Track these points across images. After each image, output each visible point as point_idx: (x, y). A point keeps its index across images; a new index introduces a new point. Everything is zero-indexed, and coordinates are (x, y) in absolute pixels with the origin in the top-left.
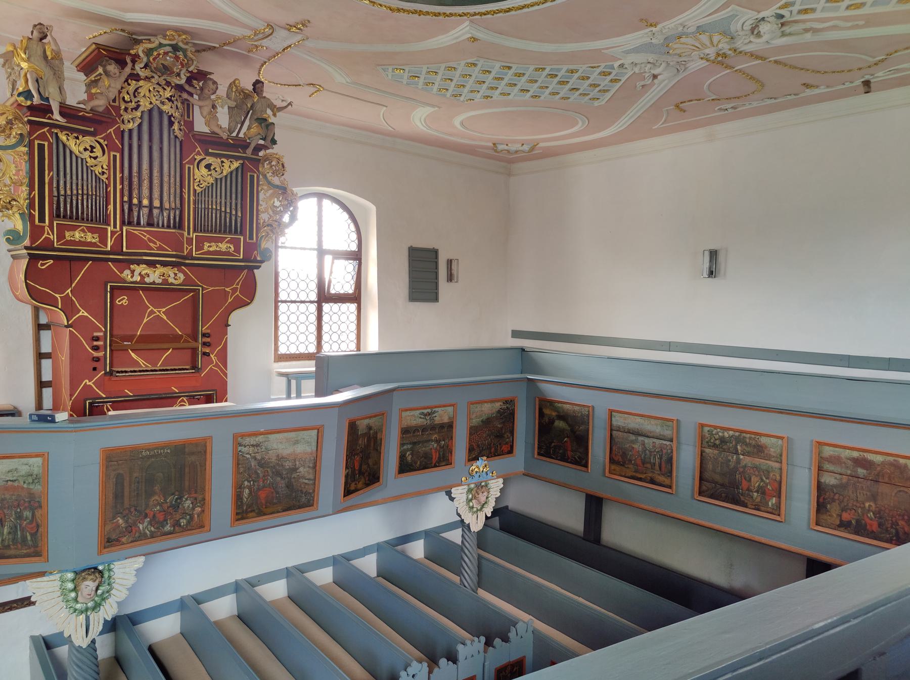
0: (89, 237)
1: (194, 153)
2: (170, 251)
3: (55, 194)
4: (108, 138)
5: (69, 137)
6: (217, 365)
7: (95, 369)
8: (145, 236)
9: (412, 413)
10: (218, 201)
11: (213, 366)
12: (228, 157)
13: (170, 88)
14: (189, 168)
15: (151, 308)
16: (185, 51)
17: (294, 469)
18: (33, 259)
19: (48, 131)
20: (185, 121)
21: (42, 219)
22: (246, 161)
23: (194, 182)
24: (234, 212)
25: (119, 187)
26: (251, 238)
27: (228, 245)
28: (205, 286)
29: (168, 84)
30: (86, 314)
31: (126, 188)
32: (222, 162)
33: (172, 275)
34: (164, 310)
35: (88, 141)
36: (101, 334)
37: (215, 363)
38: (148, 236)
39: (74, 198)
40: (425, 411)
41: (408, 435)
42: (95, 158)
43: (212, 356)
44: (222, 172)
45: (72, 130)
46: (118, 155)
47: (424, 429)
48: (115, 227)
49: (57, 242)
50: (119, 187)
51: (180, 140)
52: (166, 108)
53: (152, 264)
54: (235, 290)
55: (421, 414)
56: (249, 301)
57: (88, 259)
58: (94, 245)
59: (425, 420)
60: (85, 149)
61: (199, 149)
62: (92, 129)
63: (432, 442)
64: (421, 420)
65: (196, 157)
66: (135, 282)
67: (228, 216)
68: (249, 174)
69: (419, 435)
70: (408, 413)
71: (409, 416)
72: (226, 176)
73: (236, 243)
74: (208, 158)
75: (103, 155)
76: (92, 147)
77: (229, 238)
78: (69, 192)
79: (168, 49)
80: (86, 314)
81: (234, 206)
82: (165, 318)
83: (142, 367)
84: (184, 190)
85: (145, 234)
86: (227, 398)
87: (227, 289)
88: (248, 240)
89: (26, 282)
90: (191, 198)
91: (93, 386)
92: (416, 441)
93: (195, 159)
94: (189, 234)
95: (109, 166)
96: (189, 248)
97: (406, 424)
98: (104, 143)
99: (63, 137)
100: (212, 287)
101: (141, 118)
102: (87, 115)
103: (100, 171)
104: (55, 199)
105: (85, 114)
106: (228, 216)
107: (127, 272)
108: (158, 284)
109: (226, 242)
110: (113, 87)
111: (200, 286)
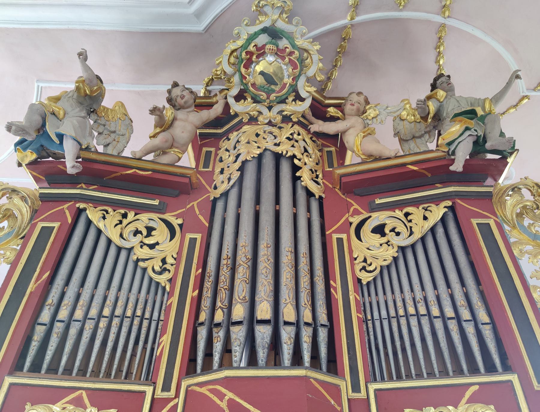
1: (347, 215)
4: (188, 216)
5: (107, 216)
8: (221, 396)
10: (419, 295)
12: (415, 202)
13: (290, 124)
14: (340, 241)
19: (68, 208)
20: (324, 172)
22: (459, 201)
23: (352, 265)
24: (466, 314)
25: (192, 293)
29: (286, 119)
31: (208, 294)
32: (407, 215)
38: (230, 395)
42: (152, 247)
44: (411, 233)
45: (116, 204)
50: (192, 293)
51: (317, 197)
60: (137, 232)
61: (356, 206)
65: (351, 220)
67: (453, 325)
72: (423, 239)
74: (374, 215)
75: (171, 240)
76: (150, 230)
77: (476, 387)
81: (460, 300)
84: (332, 282)
85: (224, 390)
90: (352, 298)
93: (351, 224)
94: (356, 388)
95: (177, 259)
98: (176, 222)
101: (241, 169)
103: (157, 268)
104: (40, 331)
105: (137, 171)
106: (453, 325)
109: (468, 402)
110: (181, 120)
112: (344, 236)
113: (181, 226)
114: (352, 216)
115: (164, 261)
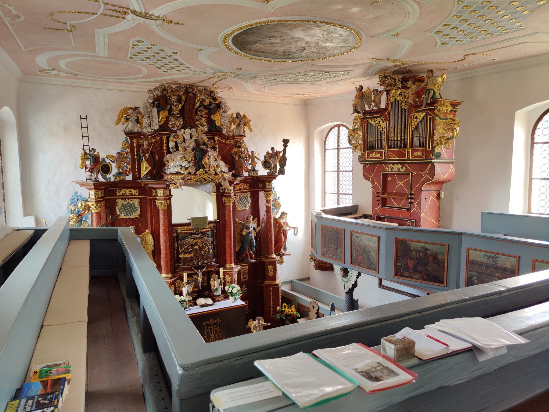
0: (378, 155)
3: (369, 141)
6: (417, 209)
7: (378, 204)
9: (479, 253)
16: (389, 76)
17: (370, 252)
18: (365, 164)
21: (364, 152)
33: (401, 168)
34: (403, 182)
35: (378, 120)
39: (375, 142)
40: (489, 254)
41: (475, 266)
42: (380, 126)
43: (415, 204)
45: (373, 118)
47: (488, 266)
48: (386, 150)
52: (398, 98)
53: (393, 164)
54: (425, 174)
55: (484, 255)
58: (379, 158)
59: (488, 260)
63: (495, 278)
64: (484, 259)
66: (389, 171)
68: (429, 117)
69: (483, 269)
70: (474, 251)
71: (474, 254)
73: (423, 151)
74: (416, 114)
78: (373, 140)
79: (384, 78)
82: (403, 186)
87: (422, 173)
88: (427, 149)
92: (480, 272)
97: (472, 258)
98: (383, 119)
107: (387, 167)
108: (397, 172)
113: (384, 119)
115: (383, 128)
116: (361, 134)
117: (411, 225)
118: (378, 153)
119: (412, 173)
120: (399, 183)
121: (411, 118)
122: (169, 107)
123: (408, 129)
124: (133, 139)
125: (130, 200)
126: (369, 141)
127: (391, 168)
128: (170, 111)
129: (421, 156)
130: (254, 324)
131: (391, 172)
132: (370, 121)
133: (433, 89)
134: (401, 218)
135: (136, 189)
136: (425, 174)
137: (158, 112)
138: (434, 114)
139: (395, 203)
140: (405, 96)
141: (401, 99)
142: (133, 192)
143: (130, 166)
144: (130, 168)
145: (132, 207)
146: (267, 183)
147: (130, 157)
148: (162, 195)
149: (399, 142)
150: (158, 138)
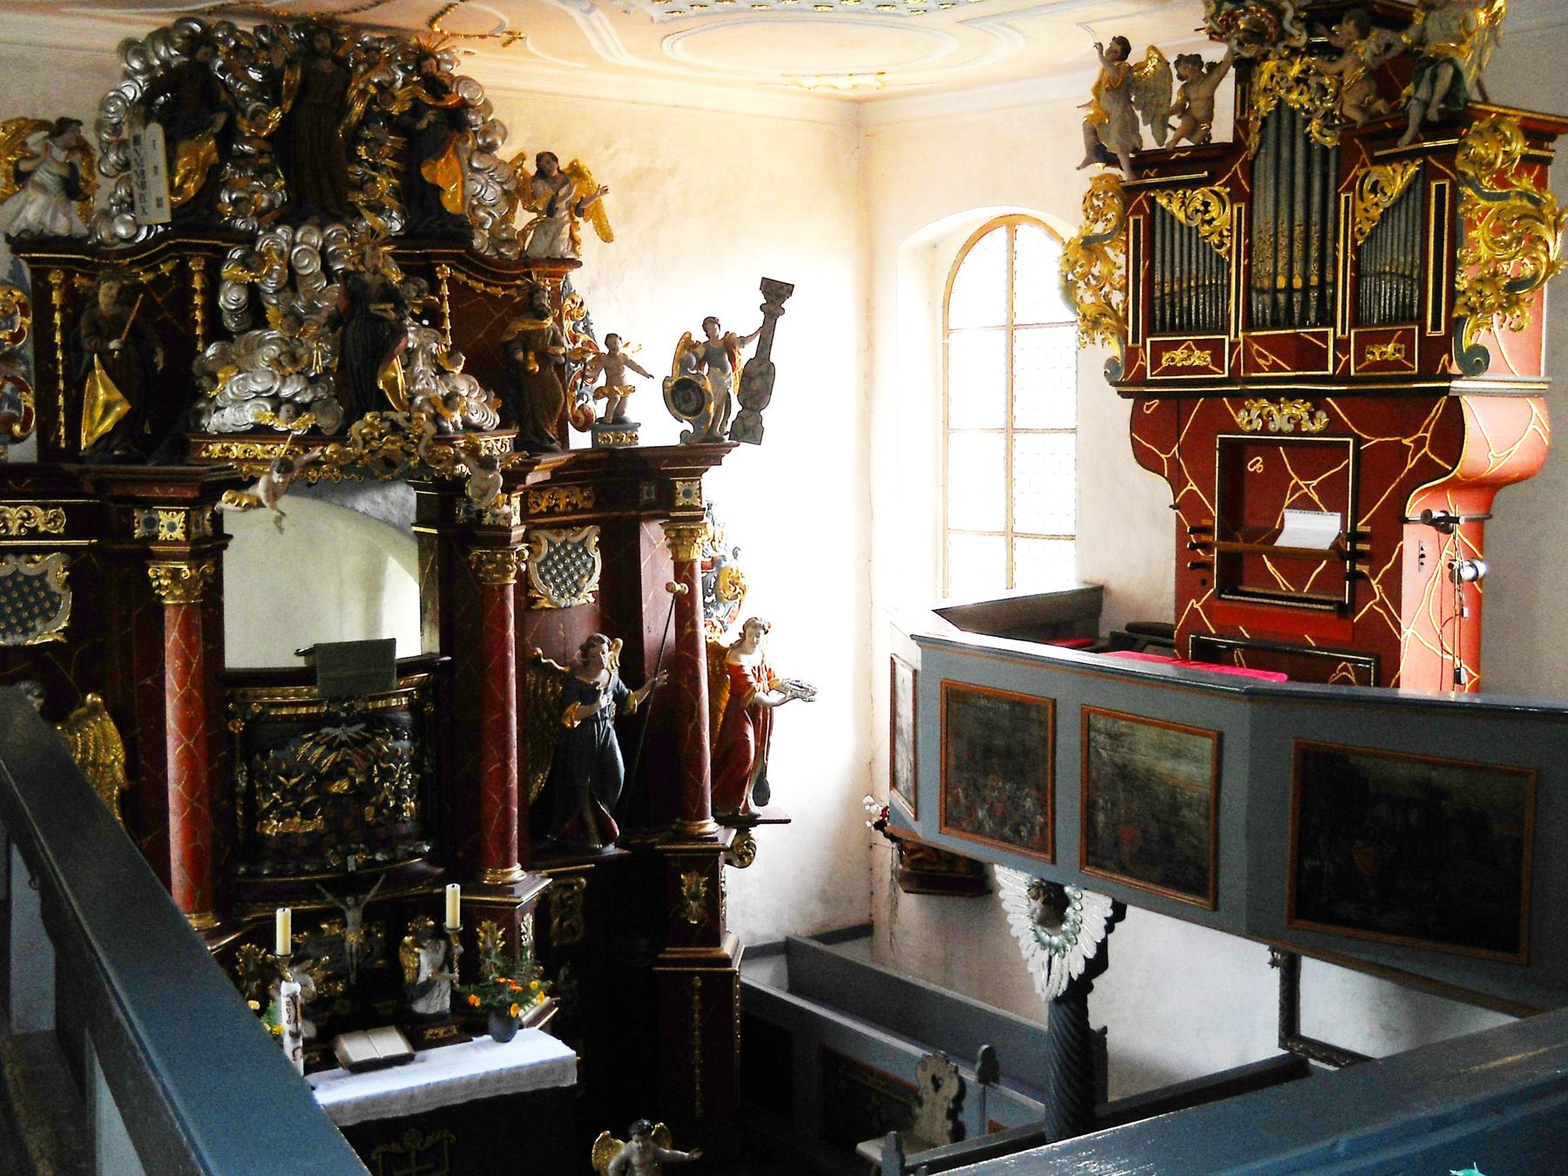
0: (1200, 358)
2: (1288, 371)
3: (1158, 294)
4: (1233, 182)
6: (1382, 604)
11: (1375, 604)
14: (1347, 198)
15: (1296, 479)
18: (1140, 399)
21: (1135, 340)
22: (1430, 158)
26: (1436, 326)
27: (1399, 346)
28: (1366, 437)
30: (1195, 488)
33: (1306, 416)
34: (1315, 483)
35: (1199, 195)
36: (1209, 523)
37: (1378, 598)
43: (1374, 583)
45: (1176, 186)
46: (1243, 205)
48: (1236, 335)
49: (1151, 372)
53: (1273, 397)
54: (1420, 443)
56: (1450, 468)
57: (1200, 394)
58: (1205, 370)
62: (1206, 174)
65: (1358, 173)
66: (1254, 432)
68: (1434, 185)
73: (1407, 338)
74: (1373, 169)
76: (1206, 204)
80: (1195, 488)
83: (1281, 589)
86: (1398, 679)
87: (1406, 442)
88: (1429, 330)
89: (1131, 436)
91: (1201, 611)
96: (1344, 359)
99: (1163, 201)
100: (1376, 438)
102: (1183, 155)
103: (1216, 242)
107: (1243, 413)
108: (1289, 434)
111: (1351, 434)
112: (1351, 195)
113: (1228, 194)
114: (1360, 168)
115: (1221, 234)
116: (1121, 260)
117: (1353, 679)
118: (1201, 345)
119: (1359, 441)
120: (1297, 487)
121: (1350, 188)
122: (220, 120)
123: (1336, 239)
124: (49, 271)
125: (24, 558)
126: (1158, 294)
127: (1260, 416)
128: (227, 137)
129: (1397, 361)
130: (623, 1152)
131: (1260, 433)
132: (1162, 201)
133: (1451, 61)
134: (1311, 647)
135: (56, 506)
136: (1420, 443)
137: (171, 142)
138: (1454, 169)
139: (1277, 576)
140: (1323, 89)
141: (1304, 98)
142: (40, 518)
143: (28, 400)
144: (28, 410)
145: (33, 592)
146: (679, 485)
147: (29, 353)
148: (178, 534)
149: (1297, 298)
150: (165, 269)
